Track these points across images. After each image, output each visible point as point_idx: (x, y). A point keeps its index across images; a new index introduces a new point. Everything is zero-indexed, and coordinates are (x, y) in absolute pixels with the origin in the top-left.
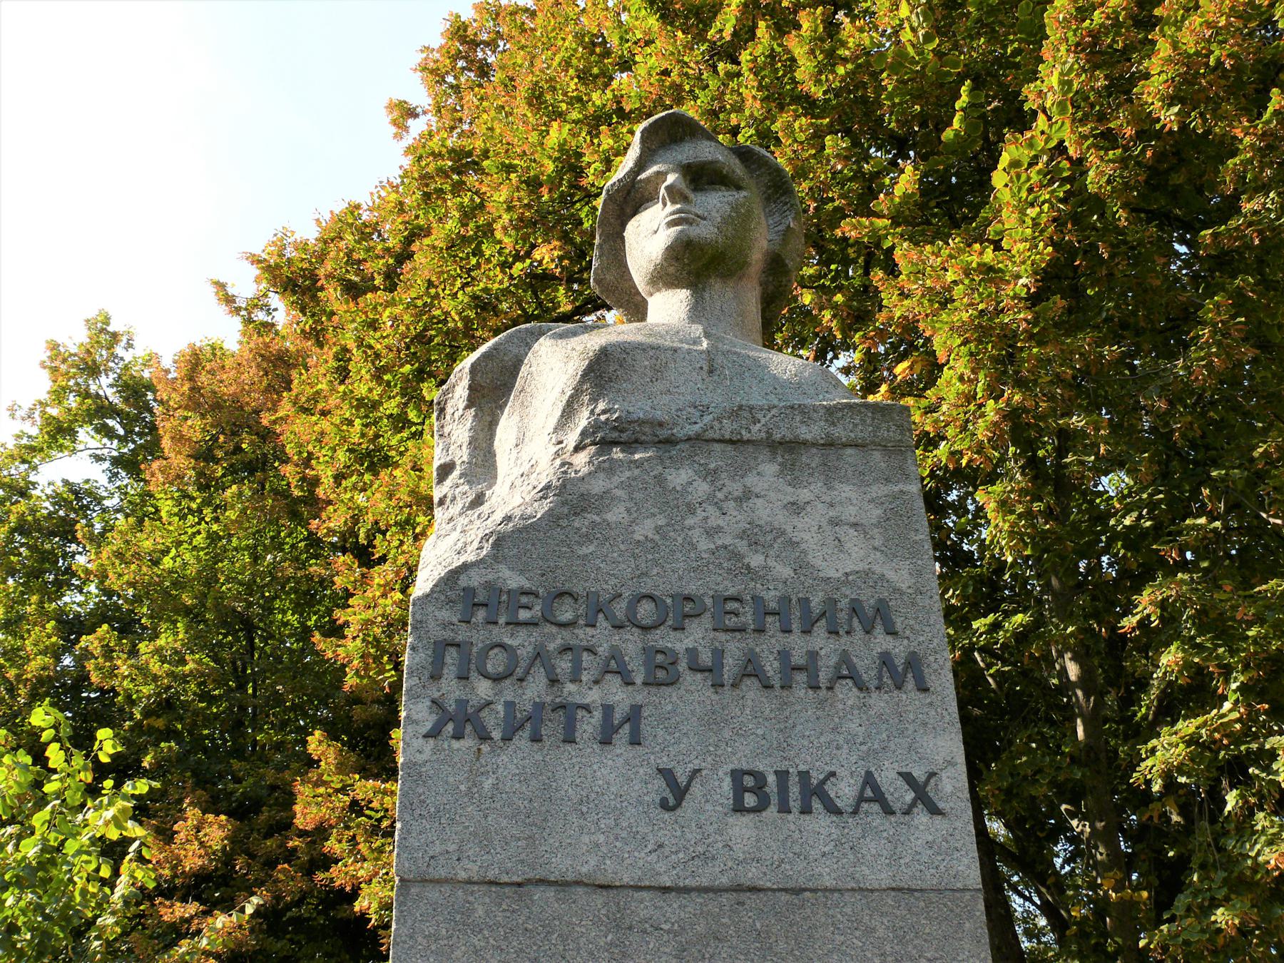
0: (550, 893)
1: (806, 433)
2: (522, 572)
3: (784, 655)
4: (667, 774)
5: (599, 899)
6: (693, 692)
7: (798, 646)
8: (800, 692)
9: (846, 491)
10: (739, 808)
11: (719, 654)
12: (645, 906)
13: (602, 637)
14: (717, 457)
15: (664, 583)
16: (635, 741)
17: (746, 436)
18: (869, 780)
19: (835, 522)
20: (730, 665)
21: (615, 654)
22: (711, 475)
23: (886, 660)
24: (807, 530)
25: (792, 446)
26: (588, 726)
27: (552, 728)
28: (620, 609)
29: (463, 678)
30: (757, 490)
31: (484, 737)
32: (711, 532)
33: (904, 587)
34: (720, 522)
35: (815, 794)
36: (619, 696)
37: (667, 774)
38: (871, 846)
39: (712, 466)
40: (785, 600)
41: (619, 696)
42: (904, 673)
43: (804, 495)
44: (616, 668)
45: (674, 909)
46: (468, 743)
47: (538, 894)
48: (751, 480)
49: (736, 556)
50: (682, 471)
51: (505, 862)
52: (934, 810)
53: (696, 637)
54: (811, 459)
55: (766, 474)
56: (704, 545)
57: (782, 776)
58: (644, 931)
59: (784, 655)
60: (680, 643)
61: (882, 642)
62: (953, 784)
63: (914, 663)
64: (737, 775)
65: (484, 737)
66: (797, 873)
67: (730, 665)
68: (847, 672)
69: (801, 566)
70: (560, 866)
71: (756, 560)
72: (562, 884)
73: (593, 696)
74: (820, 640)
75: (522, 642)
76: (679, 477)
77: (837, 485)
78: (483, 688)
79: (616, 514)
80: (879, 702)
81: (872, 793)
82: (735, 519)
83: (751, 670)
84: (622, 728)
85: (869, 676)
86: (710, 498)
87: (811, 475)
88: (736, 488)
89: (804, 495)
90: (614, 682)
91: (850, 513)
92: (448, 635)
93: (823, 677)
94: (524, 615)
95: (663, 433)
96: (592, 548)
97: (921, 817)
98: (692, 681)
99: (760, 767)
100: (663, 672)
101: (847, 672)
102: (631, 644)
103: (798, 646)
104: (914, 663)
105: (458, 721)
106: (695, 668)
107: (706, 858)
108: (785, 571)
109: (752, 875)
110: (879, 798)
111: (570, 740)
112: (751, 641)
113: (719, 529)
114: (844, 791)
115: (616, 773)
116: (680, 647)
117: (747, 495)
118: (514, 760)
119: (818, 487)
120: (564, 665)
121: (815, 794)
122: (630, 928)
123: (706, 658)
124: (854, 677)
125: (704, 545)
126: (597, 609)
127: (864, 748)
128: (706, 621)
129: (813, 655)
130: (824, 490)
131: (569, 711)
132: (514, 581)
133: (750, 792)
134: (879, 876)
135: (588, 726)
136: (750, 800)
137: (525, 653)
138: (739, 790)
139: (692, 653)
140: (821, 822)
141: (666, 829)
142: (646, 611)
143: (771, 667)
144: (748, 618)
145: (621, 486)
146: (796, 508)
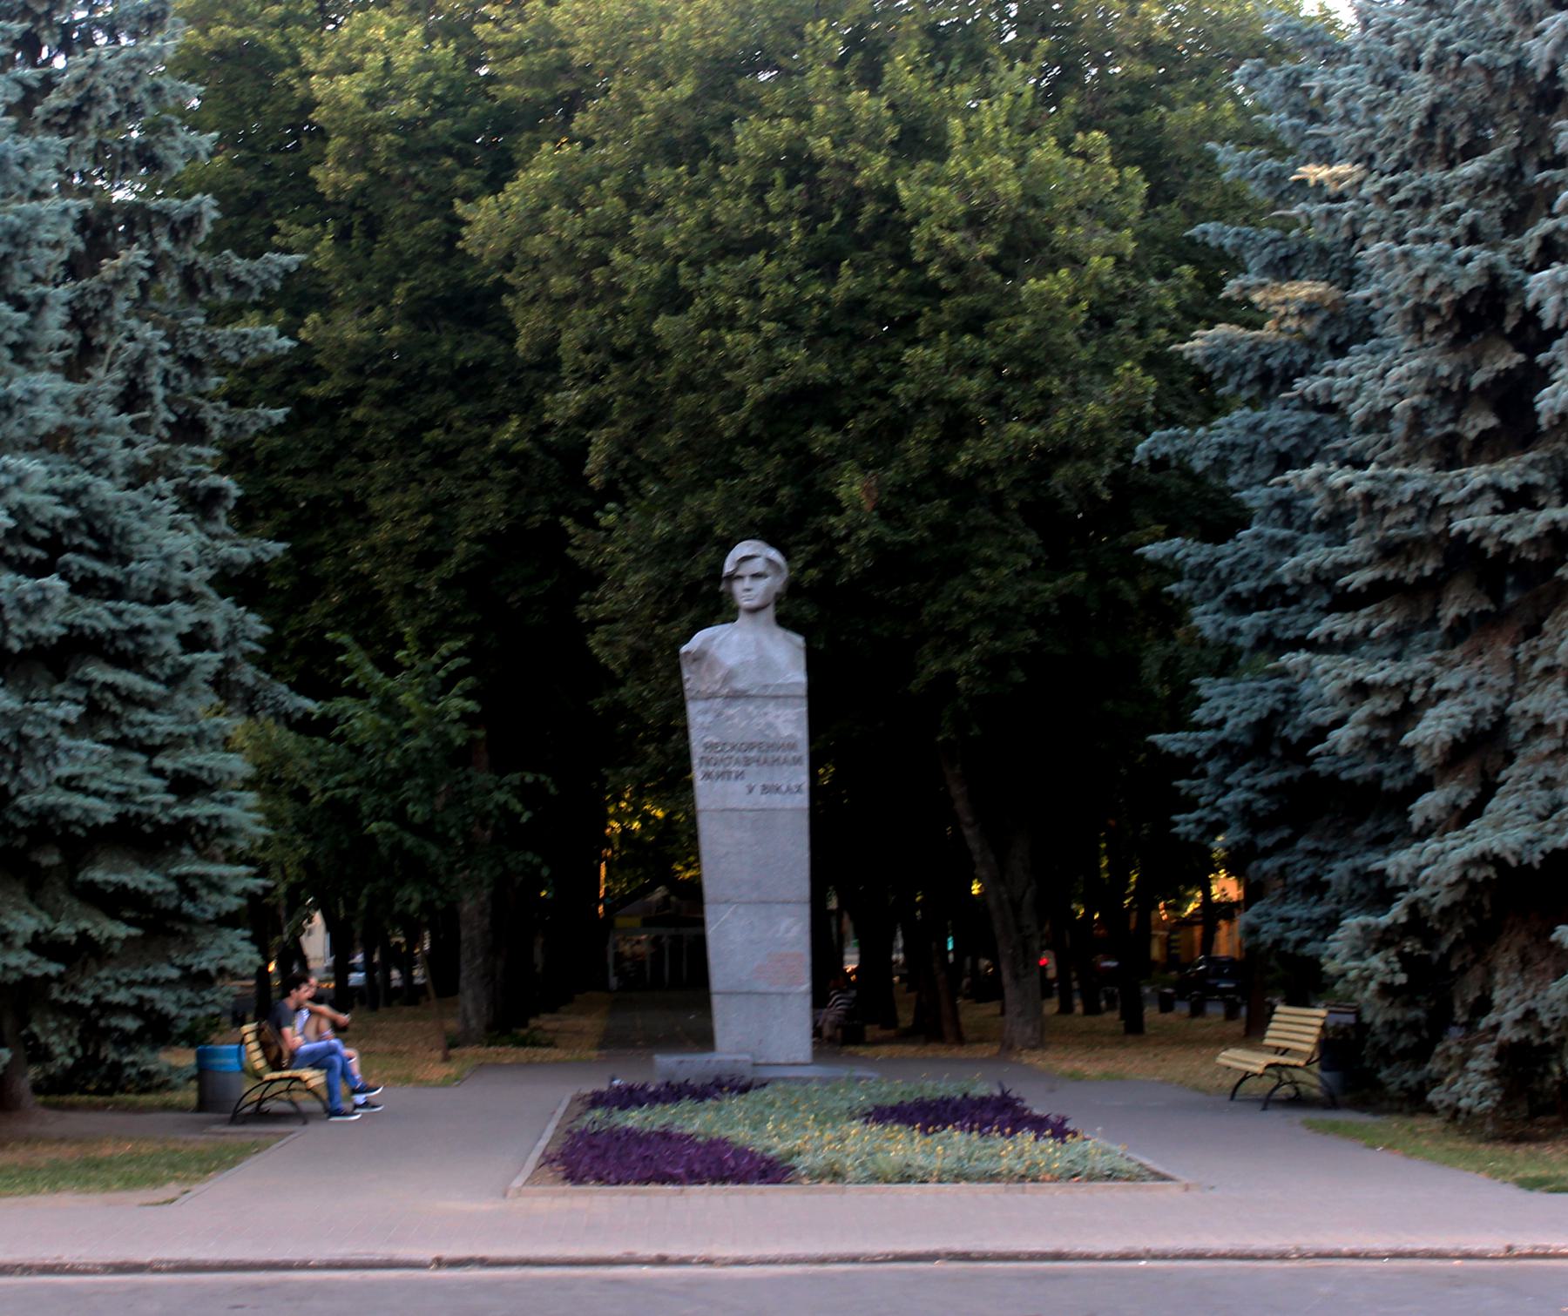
6: (754, 767)
13: (736, 755)
14: (759, 702)
24: (779, 723)
25: (776, 697)
42: (797, 761)
44: (737, 762)
53: (753, 754)
55: (771, 708)
62: (806, 786)
74: (782, 755)
81: (789, 789)
84: (740, 775)
100: (748, 762)
105: (707, 776)
115: (740, 786)
118: (719, 784)
121: (778, 789)
133: (766, 789)
140: (778, 797)
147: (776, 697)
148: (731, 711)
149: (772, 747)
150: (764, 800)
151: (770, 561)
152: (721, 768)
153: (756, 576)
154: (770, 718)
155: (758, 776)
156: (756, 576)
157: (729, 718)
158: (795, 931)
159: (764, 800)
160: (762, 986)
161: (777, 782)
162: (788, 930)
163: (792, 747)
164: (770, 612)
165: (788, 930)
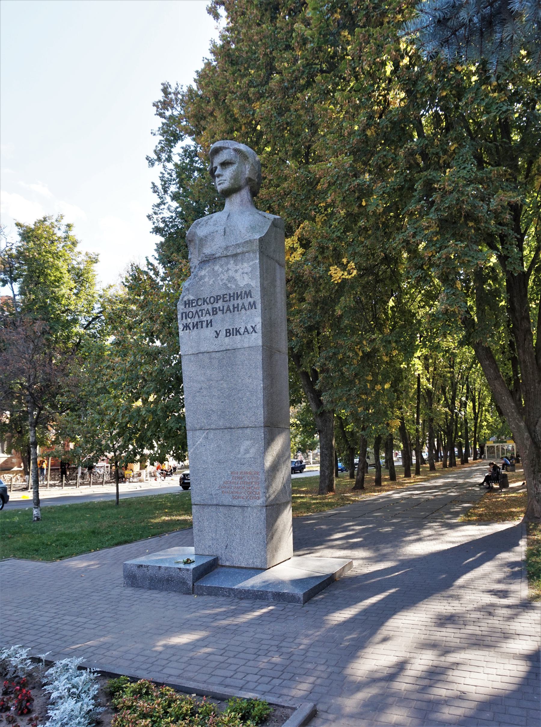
1: (239, 251)
3: (234, 305)
4: (216, 331)
5: (208, 355)
7: (236, 302)
8: (236, 312)
9: (245, 265)
10: (226, 336)
11: (223, 307)
12: (214, 355)
13: (205, 307)
15: (214, 294)
16: (211, 326)
17: (228, 254)
18: (246, 328)
19: (243, 273)
20: (225, 308)
21: (208, 310)
22: (221, 266)
23: (250, 303)
24: (238, 276)
25: (235, 255)
26: (205, 324)
27: (199, 326)
28: (208, 300)
29: (186, 318)
31: (190, 329)
32: (222, 280)
35: (238, 331)
36: (208, 318)
37: (216, 331)
38: (246, 340)
40: (234, 293)
41: (208, 318)
42: (253, 305)
45: (218, 355)
46: (188, 331)
47: (200, 355)
48: (230, 266)
49: (226, 285)
51: (195, 351)
52: (256, 332)
53: (220, 304)
54: (239, 258)
55: (231, 264)
57: (233, 329)
59: (234, 305)
60: (216, 305)
61: (250, 299)
62: (259, 327)
63: (254, 303)
64: (226, 330)
65: (190, 329)
66: (235, 346)
67: (225, 308)
68: (244, 307)
69: (237, 285)
70: (202, 350)
71: (229, 285)
72: (203, 353)
73: (204, 319)
74: (240, 301)
75: (194, 310)
76: (217, 268)
78: (189, 320)
79: (206, 279)
80: (248, 312)
82: (225, 277)
83: (228, 309)
84: (210, 324)
85: (247, 307)
86: (222, 273)
88: (226, 268)
90: (208, 315)
91: (246, 270)
92: (182, 311)
93: (240, 308)
94: (194, 305)
97: (254, 334)
98: (220, 313)
99: (231, 328)
100: (215, 312)
101: (244, 307)
102: (210, 307)
103: (236, 302)
104: (254, 303)
105: (186, 327)
106: (220, 310)
107: (222, 345)
108: (234, 287)
109: (228, 347)
110: (247, 331)
111: (202, 327)
112: (228, 303)
114: (242, 331)
115: (208, 332)
116: (217, 307)
117: (228, 269)
118: (195, 332)
119: (240, 265)
120: (200, 314)
123: (221, 308)
124: (245, 308)
126: (205, 301)
128: (222, 300)
129: (238, 304)
131: (202, 322)
132: (192, 298)
133: (229, 333)
134: (246, 345)
135: (205, 324)
136: (228, 334)
137: (194, 312)
138: (226, 333)
139: (219, 307)
140: (239, 336)
141: (217, 342)
142: (212, 299)
143: (231, 308)
144: (228, 298)
145: (208, 272)
146: (236, 271)
148: (203, 273)
149: (238, 296)
150: (227, 342)
151: (236, 150)
152: (196, 319)
153: (225, 164)
154: (231, 273)
155: (222, 322)
156: (225, 164)
157: (202, 278)
158: (253, 451)
159: (227, 342)
160: (227, 499)
161: (237, 326)
162: (247, 451)
163: (249, 294)
164: (245, 193)
165: (247, 451)
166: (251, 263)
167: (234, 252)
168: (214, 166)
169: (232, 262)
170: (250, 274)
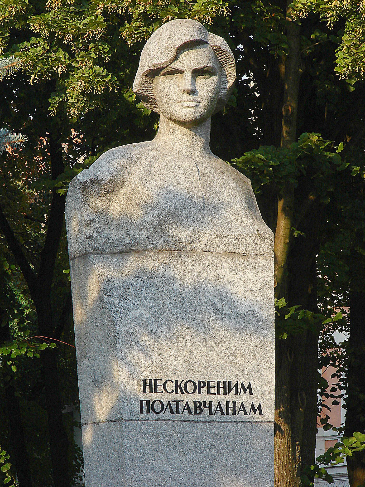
0: (163, 422)
2: (149, 311)
9: (250, 275)
30: (221, 276)
33: (264, 316)
34: (209, 290)
39: (207, 264)
43: (236, 278)
49: (213, 304)
50: (197, 267)
54: (239, 260)
56: (204, 300)
58: (187, 434)
71: (220, 306)
77: (246, 273)
87: (239, 268)
89: (236, 278)
91: (249, 285)
95: (189, 247)
96: (169, 301)
113: (209, 293)
122: (184, 433)
125: (204, 300)
127: (247, 376)
130: (243, 275)
147: (231, 254)
166: (261, 275)
167: (230, 249)
168: (177, 65)
169: (226, 265)
170: (257, 294)
